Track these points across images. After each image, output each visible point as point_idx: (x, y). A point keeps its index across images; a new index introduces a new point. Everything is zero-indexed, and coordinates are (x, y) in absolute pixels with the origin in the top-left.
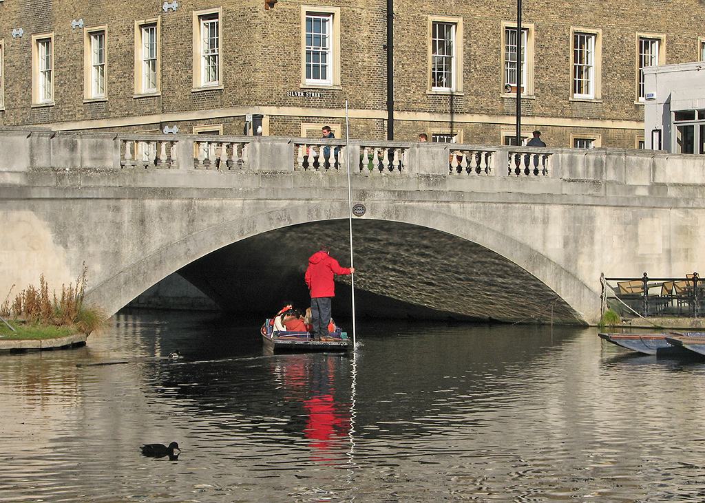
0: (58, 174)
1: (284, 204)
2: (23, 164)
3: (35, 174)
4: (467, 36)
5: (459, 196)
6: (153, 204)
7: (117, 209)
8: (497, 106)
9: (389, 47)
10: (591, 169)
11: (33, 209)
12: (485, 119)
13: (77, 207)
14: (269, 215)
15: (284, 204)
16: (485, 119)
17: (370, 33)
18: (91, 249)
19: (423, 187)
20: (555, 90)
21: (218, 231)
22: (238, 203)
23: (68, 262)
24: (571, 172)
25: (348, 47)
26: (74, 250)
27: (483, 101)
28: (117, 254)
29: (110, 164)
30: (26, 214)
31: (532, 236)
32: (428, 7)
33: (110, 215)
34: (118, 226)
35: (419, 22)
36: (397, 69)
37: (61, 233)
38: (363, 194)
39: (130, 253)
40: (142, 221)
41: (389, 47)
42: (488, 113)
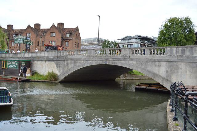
0: (57, 57)
5: (132, 60)
6: (69, 61)
7: (64, 62)
10: (180, 52)
13: (59, 62)
15: (91, 61)
18: (61, 68)
19: (122, 58)
22: (83, 61)
23: (58, 70)
24: (170, 53)
26: (58, 68)
31: (155, 70)
33: (63, 63)
34: (64, 64)
37: (58, 66)
38: (107, 59)
39: (66, 69)
40: (68, 64)
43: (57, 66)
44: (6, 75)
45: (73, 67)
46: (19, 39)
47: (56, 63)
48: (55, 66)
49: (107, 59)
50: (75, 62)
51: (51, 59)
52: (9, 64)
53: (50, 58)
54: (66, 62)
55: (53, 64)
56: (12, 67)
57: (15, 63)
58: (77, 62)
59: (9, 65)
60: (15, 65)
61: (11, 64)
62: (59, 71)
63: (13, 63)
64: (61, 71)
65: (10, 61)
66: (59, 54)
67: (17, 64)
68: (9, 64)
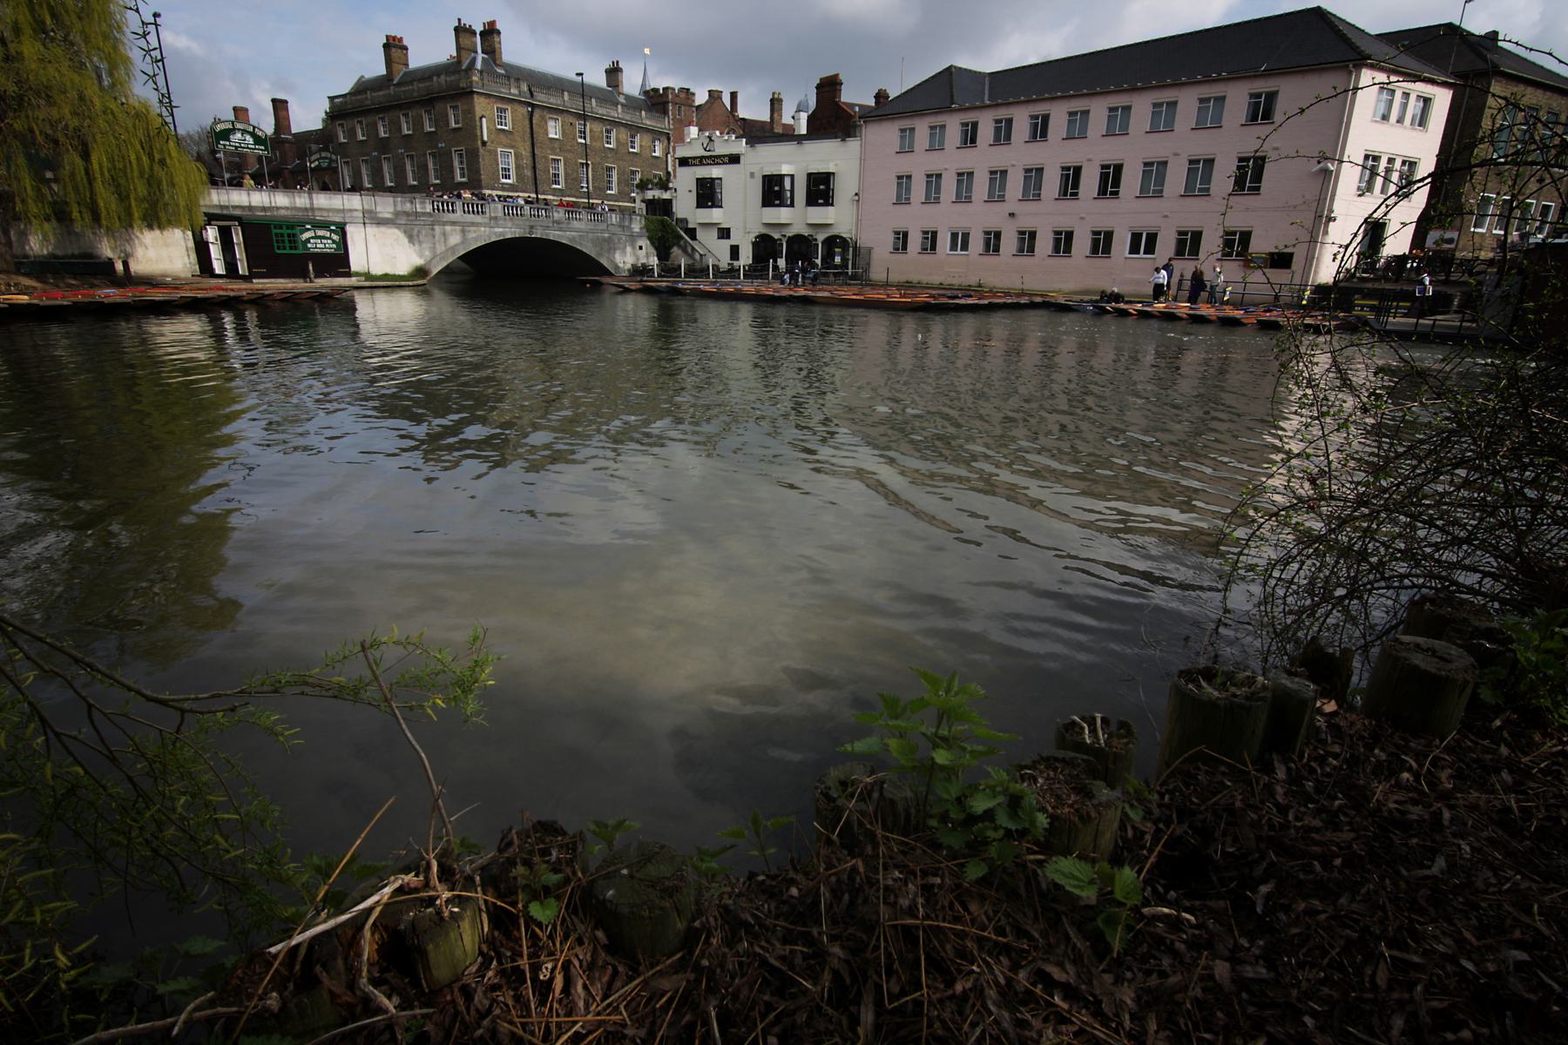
0: (407, 214)
1: (501, 230)
2: (391, 209)
3: (397, 214)
4: (565, 164)
6: (448, 228)
7: (433, 229)
8: (577, 194)
9: (534, 168)
11: (398, 228)
12: (574, 199)
14: (496, 233)
15: (501, 230)
16: (574, 199)
17: (527, 161)
18: (424, 245)
20: (600, 189)
21: (476, 239)
23: (415, 250)
25: (518, 167)
26: (417, 245)
27: (573, 192)
28: (434, 248)
29: (428, 210)
30: (396, 231)
32: (549, 152)
34: (434, 237)
35: (546, 158)
36: (538, 177)
37: (411, 238)
39: (440, 248)
41: (534, 168)
42: (576, 197)
43: (410, 242)
44: (320, 274)
45: (462, 243)
46: (239, 135)
47: (405, 232)
48: (406, 240)
49: (532, 227)
50: (463, 231)
51: (387, 219)
52: (306, 236)
53: (380, 215)
54: (437, 228)
55: (395, 236)
56: (322, 246)
57: (328, 234)
58: (469, 231)
59: (308, 240)
60: (329, 241)
61: (312, 238)
62: (421, 256)
63: (320, 233)
64: (427, 253)
65: (309, 227)
66: (408, 205)
67: (335, 237)
68: (306, 236)
